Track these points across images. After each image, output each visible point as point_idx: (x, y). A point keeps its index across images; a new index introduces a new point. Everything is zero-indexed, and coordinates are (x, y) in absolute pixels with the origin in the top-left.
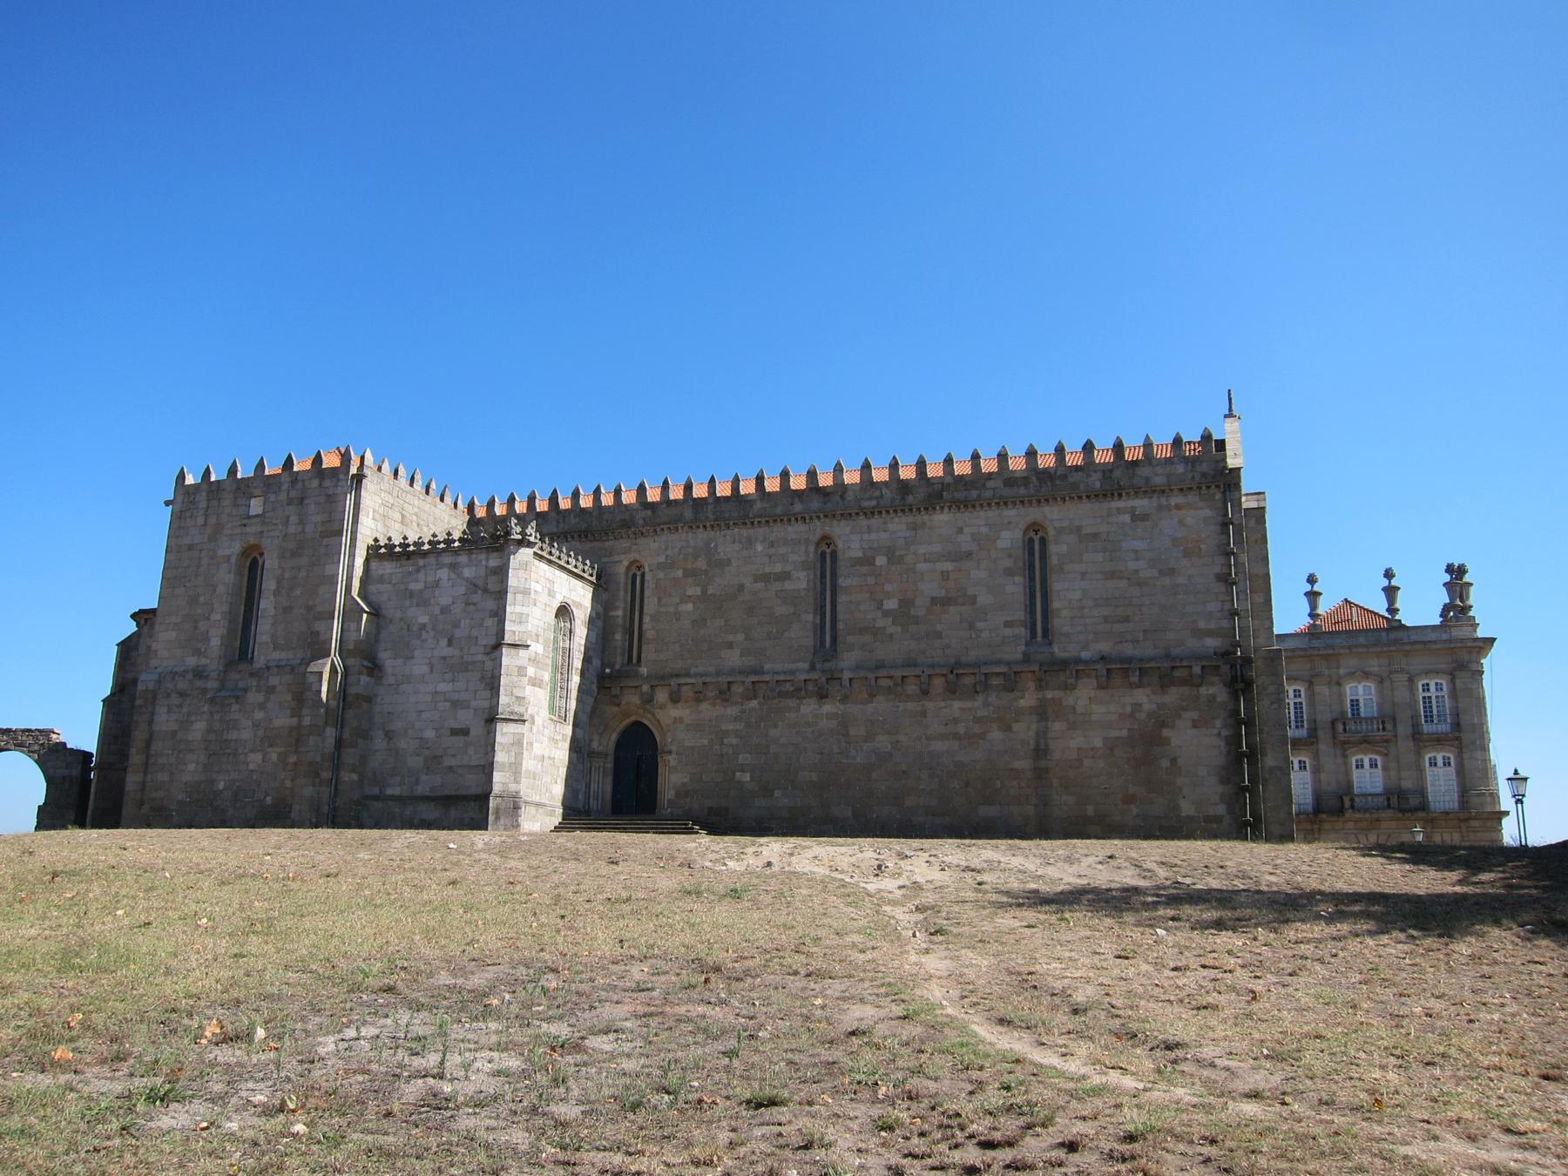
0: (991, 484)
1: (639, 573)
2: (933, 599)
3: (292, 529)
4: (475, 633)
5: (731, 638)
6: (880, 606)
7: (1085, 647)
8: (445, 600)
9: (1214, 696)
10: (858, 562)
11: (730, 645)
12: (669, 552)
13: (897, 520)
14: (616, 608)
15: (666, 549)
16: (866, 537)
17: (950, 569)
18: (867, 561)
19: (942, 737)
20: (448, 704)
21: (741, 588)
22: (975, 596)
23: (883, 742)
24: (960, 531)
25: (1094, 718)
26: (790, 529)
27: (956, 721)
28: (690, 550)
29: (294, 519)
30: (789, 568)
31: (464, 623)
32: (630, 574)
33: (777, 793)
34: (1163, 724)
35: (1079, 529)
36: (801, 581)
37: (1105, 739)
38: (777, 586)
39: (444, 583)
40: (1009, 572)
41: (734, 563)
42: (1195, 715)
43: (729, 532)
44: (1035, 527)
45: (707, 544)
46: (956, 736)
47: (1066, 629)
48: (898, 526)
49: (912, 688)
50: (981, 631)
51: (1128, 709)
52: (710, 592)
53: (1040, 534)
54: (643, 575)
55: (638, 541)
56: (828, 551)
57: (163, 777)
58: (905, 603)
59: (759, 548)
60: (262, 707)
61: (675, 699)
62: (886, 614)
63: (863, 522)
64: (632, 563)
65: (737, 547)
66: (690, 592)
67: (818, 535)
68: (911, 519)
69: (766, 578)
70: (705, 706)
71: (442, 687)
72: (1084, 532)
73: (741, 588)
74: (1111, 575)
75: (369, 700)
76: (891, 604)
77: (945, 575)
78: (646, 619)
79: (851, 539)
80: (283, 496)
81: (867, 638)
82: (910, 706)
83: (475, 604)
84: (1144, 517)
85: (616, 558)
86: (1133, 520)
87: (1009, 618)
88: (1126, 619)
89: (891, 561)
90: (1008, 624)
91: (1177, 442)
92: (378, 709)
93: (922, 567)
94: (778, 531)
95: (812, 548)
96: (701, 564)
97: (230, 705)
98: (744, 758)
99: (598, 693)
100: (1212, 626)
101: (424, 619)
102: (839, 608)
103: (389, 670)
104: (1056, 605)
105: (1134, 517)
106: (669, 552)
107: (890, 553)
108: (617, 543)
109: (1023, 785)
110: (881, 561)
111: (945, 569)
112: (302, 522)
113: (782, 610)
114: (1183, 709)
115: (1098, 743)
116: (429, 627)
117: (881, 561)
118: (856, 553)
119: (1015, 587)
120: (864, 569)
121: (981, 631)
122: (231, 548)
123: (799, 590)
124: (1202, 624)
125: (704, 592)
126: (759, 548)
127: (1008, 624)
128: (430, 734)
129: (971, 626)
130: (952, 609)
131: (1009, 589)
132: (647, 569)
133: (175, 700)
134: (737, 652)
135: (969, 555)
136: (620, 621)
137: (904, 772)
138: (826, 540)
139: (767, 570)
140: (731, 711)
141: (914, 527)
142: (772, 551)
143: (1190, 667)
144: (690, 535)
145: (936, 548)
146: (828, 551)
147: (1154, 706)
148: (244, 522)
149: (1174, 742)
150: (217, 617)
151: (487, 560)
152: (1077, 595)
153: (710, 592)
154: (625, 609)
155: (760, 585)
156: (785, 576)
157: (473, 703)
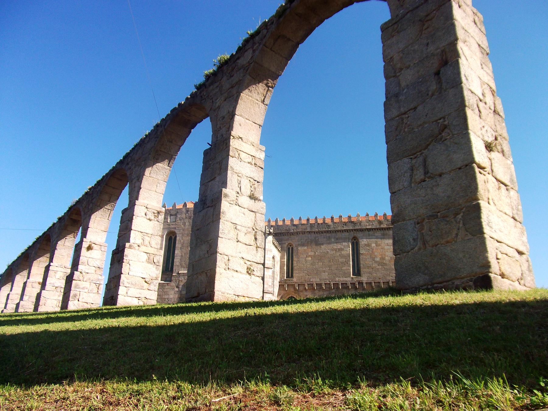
1: (291, 247)
5: (324, 269)
12: (302, 240)
13: (378, 232)
15: (301, 240)
26: (343, 234)
28: (309, 240)
43: (322, 234)
45: (315, 238)
54: (292, 248)
55: (291, 237)
56: (355, 242)
58: (383, 258)
62: (376, 262)
64: (288, 244)
67: (352, 236)
68: (382, 232)
76: (378, 259)
78: (295, 263)
81: (370, 270)
85: (284, 242)
91: (376, 215)
97: (165, 286)
106: (302, 240)
108: (283, 237)
132: (294, 246)
144: (309, 235)
146: (355, 242)
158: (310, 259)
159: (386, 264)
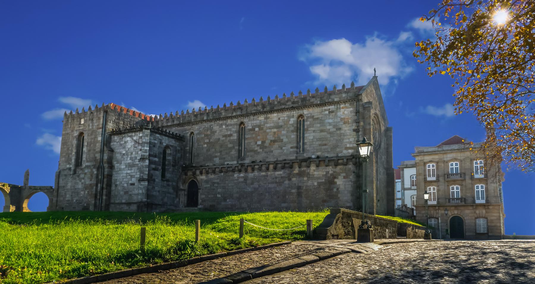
2: (271, 141)
3: (90, 128)
4: (136, 156)
5: (216, 154)
6: (256, 143)
7: (313, 154)
8: (129, 146)
9: (350, 168)
10: (250, 130)
11: (216, 157)
13: (261, 116)
14: (187, 147)
15: (200, 128)
16: (253, 122)
17: (276, 131)
18: (253, 129)
19: (272, 183)
20: (130, 177)
21: (219, 139)
22: (283, 139)
23: (256, 185)
24: (279, 119)
25: (315, 176)
26: (232, 121)
27: (276, 178)
29: (91, 125)
30: (232, 133)
31: (134, 153)
32: (192, 136)
33: (228, 200)
34: (335, 178)
36: (235, 137)
37: (318, 183)
38: (228, 138)
39: (129, 142)
40: (292, 131)
41: (217, 132)
42: (344, 174)
44: (301, 116)
46: (276, 183)
47: (308, 148)
48: (262, 118)
50: (284, 150)
51: (325, 173)
52: (211, 141)
53: (303, 118)
56: (243, 127)
57: (62, 199)
58: (263, 142)
59: (224, 127)
60: (83, 179)
61: (201, 173)
62: (258, 145)
63: (252, 117)
65: (218, 127)
66: (206, 141)
69: (225, 136)
70: (209, 175)
71: (129, 172)
72: (314, 118)
73: (219, 139)
74: (322, 131)
76: (259, 143)
77: (275, 133)
79: (249, 123)
80: (88, 118)
81: (252, 153)
82: (264, 174)
83: (136, 147)
84: (332, 112)
87: (292, 146)
88: (325, 145)
89: (259, 130)
90: (292, 148)
92: (113, 178)
93: (268, 131)
94: (229, 121)
96: (209, 133)
98: (219, 190)
99: (182, 172)
100: (351, 146)
101: (124, 152)
102: (246, 145)
103: (116, 167)
104: (306, 141)
105: (330, 112)
107: (259, 126)
111: (274, 131)
112: (93, 126)
113: (230, 145)
114: (341, 173)
115: (316, 184)
116: (125, 154)
117: (257, 129)
119: (293, 136)
120: (252, 132)
121: (284, 150)
122: (76, 134)
123: (234, 139)
124: (348, 146)
125: (209, 141)
126: (224, 127)
127: (292, 148)
128: (125, 185)
129: (281, 149)
130: (276, 143)
131: (292, 136)
133: (64, 177)
134: (218, 158)
135: (281, 126)
136: (188, 151)
137: (261, 194)
138: (242, 123)
139: (226, 134)
140: (216, 176)
141: (266, 118)
142: (228, 128)
143: (343, 159)
145: (272, 125)
146: (243, 127)
147: (333, 172)
148: (80, 126)
149: (338, 183)
150: (74, 153)
151: (139, 134)
152: (311, 138)
153: (211, 141)
154: (190, 147)
155: (224, 138)
156: (231, 135)
157: (136, 176)
158: (206, 145)
159: (266, 147)
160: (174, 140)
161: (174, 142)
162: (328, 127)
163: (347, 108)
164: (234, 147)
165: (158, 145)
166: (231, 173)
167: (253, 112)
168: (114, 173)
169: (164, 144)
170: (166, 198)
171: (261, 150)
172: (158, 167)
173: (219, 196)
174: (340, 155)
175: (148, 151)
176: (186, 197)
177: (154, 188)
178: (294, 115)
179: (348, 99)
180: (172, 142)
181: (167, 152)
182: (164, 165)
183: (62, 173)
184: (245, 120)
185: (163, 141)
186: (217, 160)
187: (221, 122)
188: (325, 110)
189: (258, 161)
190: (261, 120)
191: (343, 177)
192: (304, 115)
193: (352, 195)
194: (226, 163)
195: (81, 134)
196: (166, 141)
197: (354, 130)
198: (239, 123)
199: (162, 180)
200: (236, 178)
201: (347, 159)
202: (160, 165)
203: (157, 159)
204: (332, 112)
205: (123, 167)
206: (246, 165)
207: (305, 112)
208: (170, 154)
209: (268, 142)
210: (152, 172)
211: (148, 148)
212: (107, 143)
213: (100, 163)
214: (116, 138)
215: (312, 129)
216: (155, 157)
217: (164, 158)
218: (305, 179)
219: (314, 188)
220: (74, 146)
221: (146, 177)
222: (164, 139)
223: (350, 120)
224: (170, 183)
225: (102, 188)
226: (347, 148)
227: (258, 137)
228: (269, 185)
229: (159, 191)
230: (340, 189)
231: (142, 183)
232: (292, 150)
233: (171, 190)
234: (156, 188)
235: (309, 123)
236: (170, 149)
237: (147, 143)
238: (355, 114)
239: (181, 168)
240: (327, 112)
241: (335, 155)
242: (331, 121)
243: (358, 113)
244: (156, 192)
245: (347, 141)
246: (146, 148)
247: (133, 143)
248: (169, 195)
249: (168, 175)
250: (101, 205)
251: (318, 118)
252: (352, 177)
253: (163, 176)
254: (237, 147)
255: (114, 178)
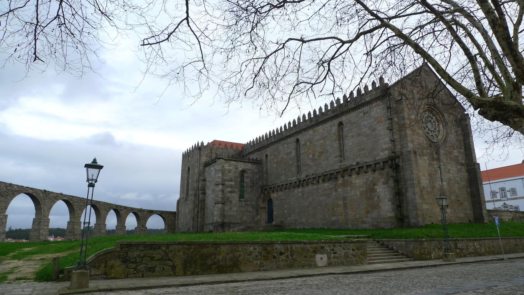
0: (329, 113)
2: (319, 153)
10: (304, 145)
18: (305, 144)
22: (328, 149)
24: (324, 130)
26: (291, 139)
27: (325, 190)
33: (292, 216)
34: (375, 184)
35: (350, 121)
36: (293, 154)
39: (213, 171)
48: (311, 132)
49: (315, 182)
58: (314, 155)
59: (286, 146)
61: (273, 192)
74: (359, 135)
75: (204, 201)
76: (311, 156)
79: (303, 138)
82: (315, 187)
86: (364, 115)
88: (363, 149)
89: (310, 143)
90: (336, 157)
93: (316, 143)
95: (295, 144)
98: (286, 206)
101: (210, 180)
103: (207, 193)
109: (341, 209)
110: (308, 143)
113: (291, 162)
115: (358, 193)
117: (308, 143)
118: (303, 143)
119: (336, 145)
125: (277, 161)
126: (286, 146)
127: (336, 157)
129: (328, 159)
134: (283, 176)
136: (265, 171)
141: (314, 132)
149: (378, 190)
150: (185, 185)
152: (351, 144)
156: (290, 153)
160: (250, 164)
161: (251, 166)
162: (364, 130)
163: (378, 105)
164: (293, 163)
165: (234, 170)
166: (292, 189)
167: (304, 128)
168: (206, 198)
169: (240, 169)
170: (245, 216)
171: (313, 163)
172: (235, 189)
173: (286, 212)
174: (377, 158)
175: (221, 177)
176: (267, 214)
177: (232, 208)
178: (335, 123)
179: (379, 95)
180: (249, 166)
181: (245, 175)
182: (242, 186)
183: (181, 201)
184: (299, 137)
185: (239, 166)
186: (283, 178)
187: (283, 142)
188: (360, 113)
189: (311, 175)
190: (310, 134)
191: (381, 183)
192: (343, 122)
193: (393, 204)
194: (289, 179)
195: (189, 168)
196: (241, 166)
197: (388, 129)
198: (295, 140)
199: (240, 201)
200: (296, 194)
201: (384, 162)
202: (236, 188)
203: (233, 183)
204: (366, 113)
205: (210, 192)
206: (302, 180)
207: (344, 119)
208: (248, 177)
209: (317, 154)
210: (228, 195)
211: (221, 175)
212: (202, 173)
213: (196, 191)
214: (207, 169)
215: (350, 134)
216: (231, 181)
217: (242, 181)
218: (349, 188)
219: (357, 198)
220: (186, 178)
221: (220, 200)
222: (240, 165)
223: (383, 119)
224: (249, 203)
225: (198, 212)
226: (383, 150)
227: (310, 151)
228: (320, 198)
229: (237, 211)
230: (380, 197)
231: (217, 205)
232: (336, 159)
233: (250, 209)
234: (234, 209)
235: (347, 129)
236: (247, 172)
237: (220, 170)
238: (386, 110)
239: (260, 188)
240: (362, 114)
241: (373, 159)
242: (366, 123)
243: (389, 110)
244: (233, 211)
245: (382, 141)
246: (219, 175)
247: (215, 171)
248: (248, 214)
249: (246, 196)
250: (197, 226)
251: (354, 122)
252: (391, 183)
253: (241, 196)
254: (296, 164)
255: (206, 202)
